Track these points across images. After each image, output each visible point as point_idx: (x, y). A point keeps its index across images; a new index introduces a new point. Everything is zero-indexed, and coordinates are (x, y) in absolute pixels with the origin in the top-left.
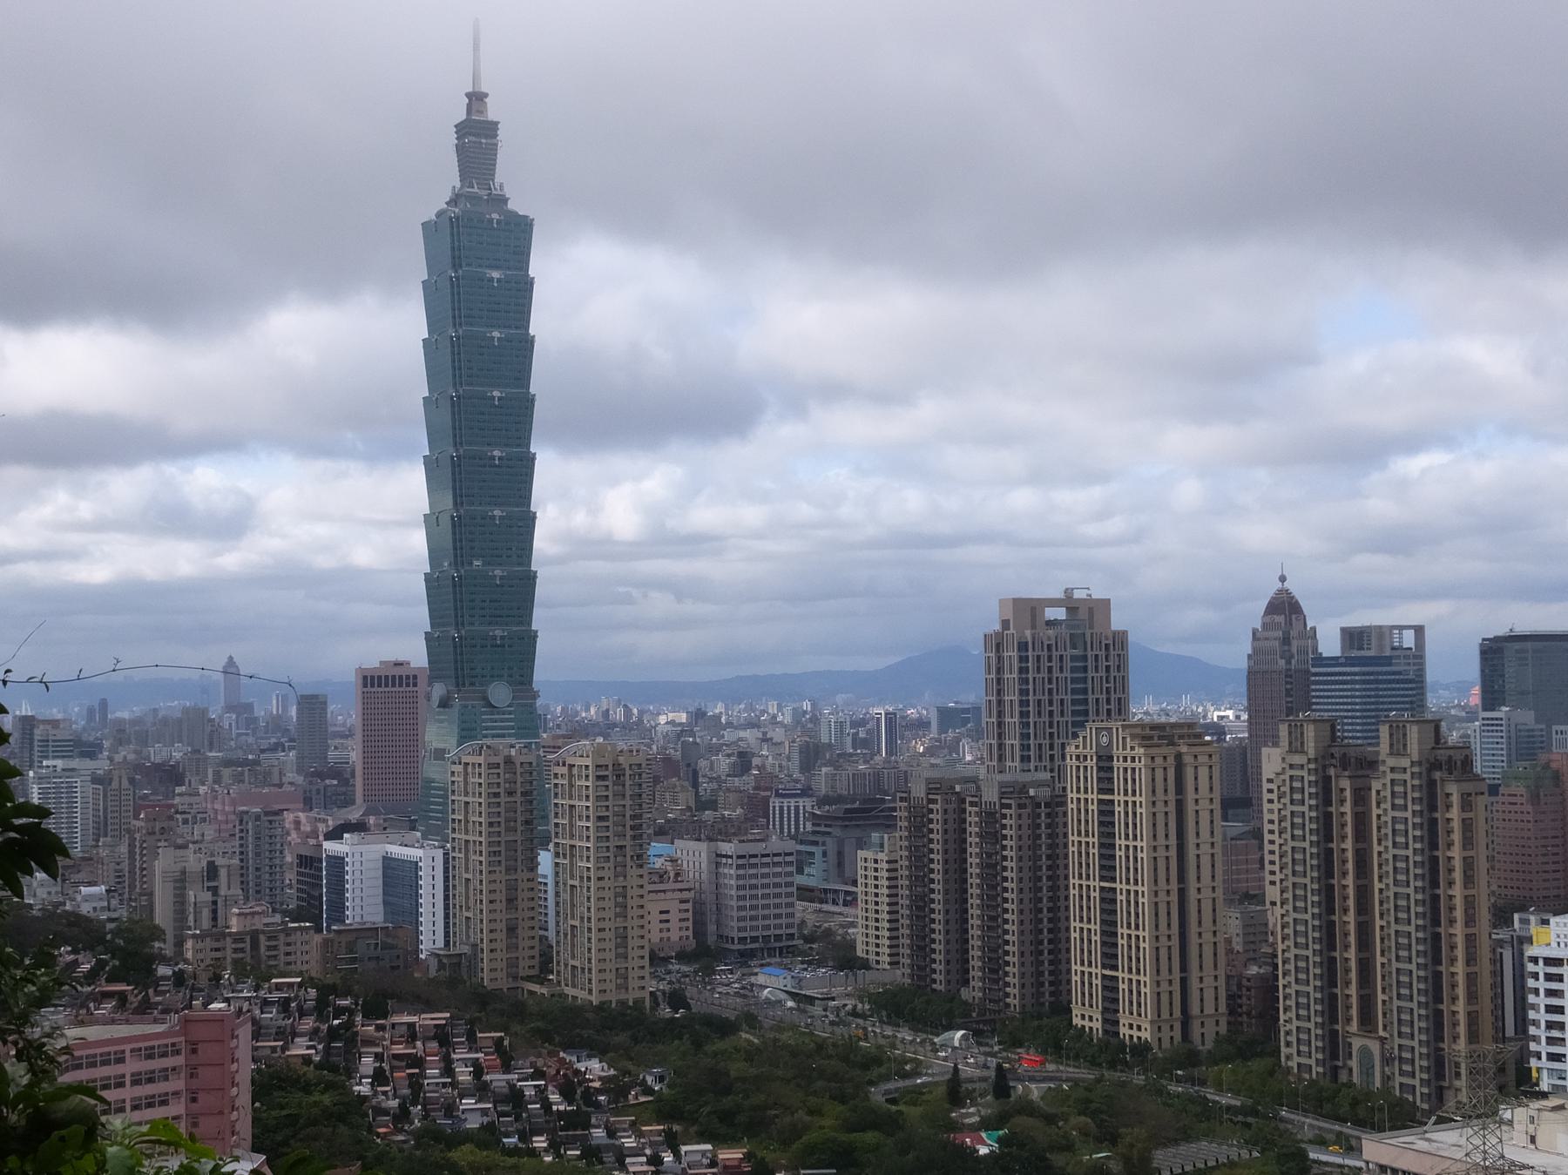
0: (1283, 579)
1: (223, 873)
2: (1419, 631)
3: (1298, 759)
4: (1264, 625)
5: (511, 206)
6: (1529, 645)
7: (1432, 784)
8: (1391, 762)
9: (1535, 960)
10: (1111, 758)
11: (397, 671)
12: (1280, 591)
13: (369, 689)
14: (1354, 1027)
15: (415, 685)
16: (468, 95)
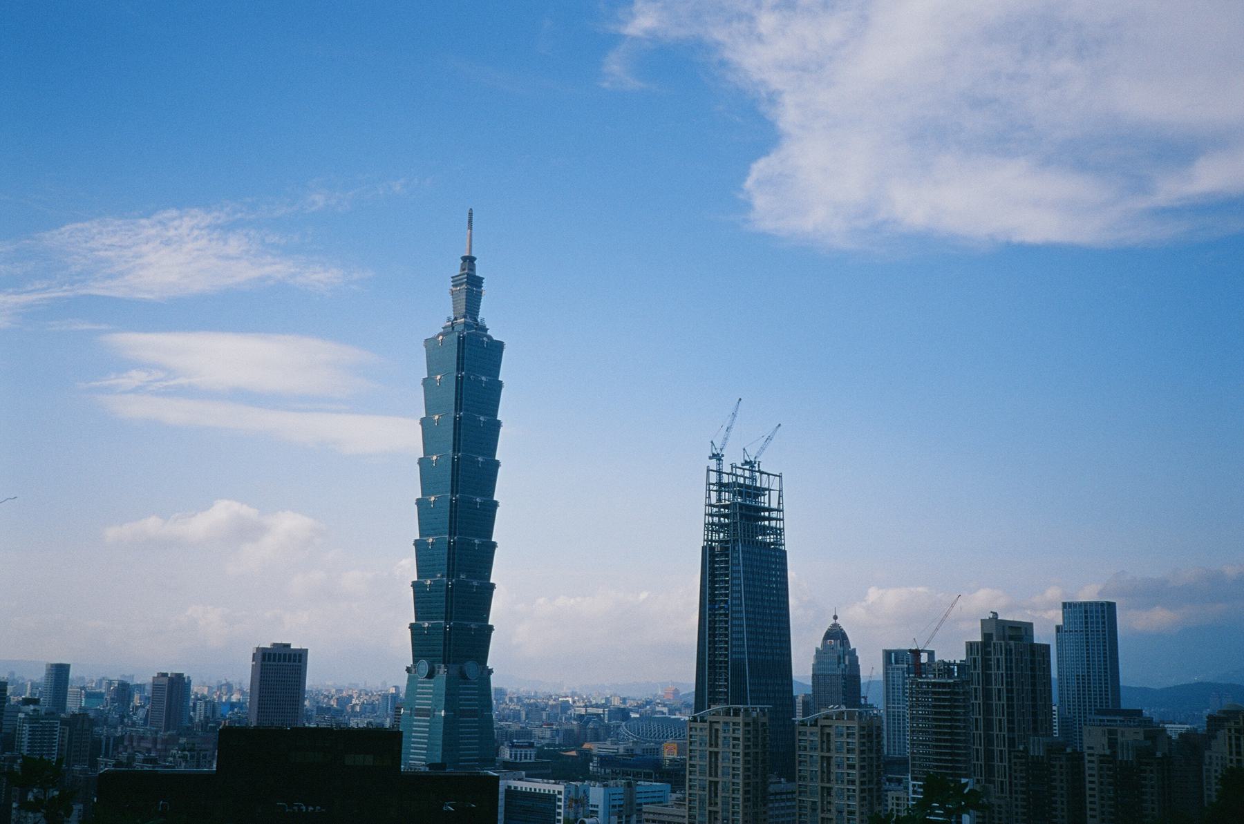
0: (835, 618)
2: (931, 654)
4: (824, 644)
5: (489, 333)
12: (835, 625)
16: (464, 259)
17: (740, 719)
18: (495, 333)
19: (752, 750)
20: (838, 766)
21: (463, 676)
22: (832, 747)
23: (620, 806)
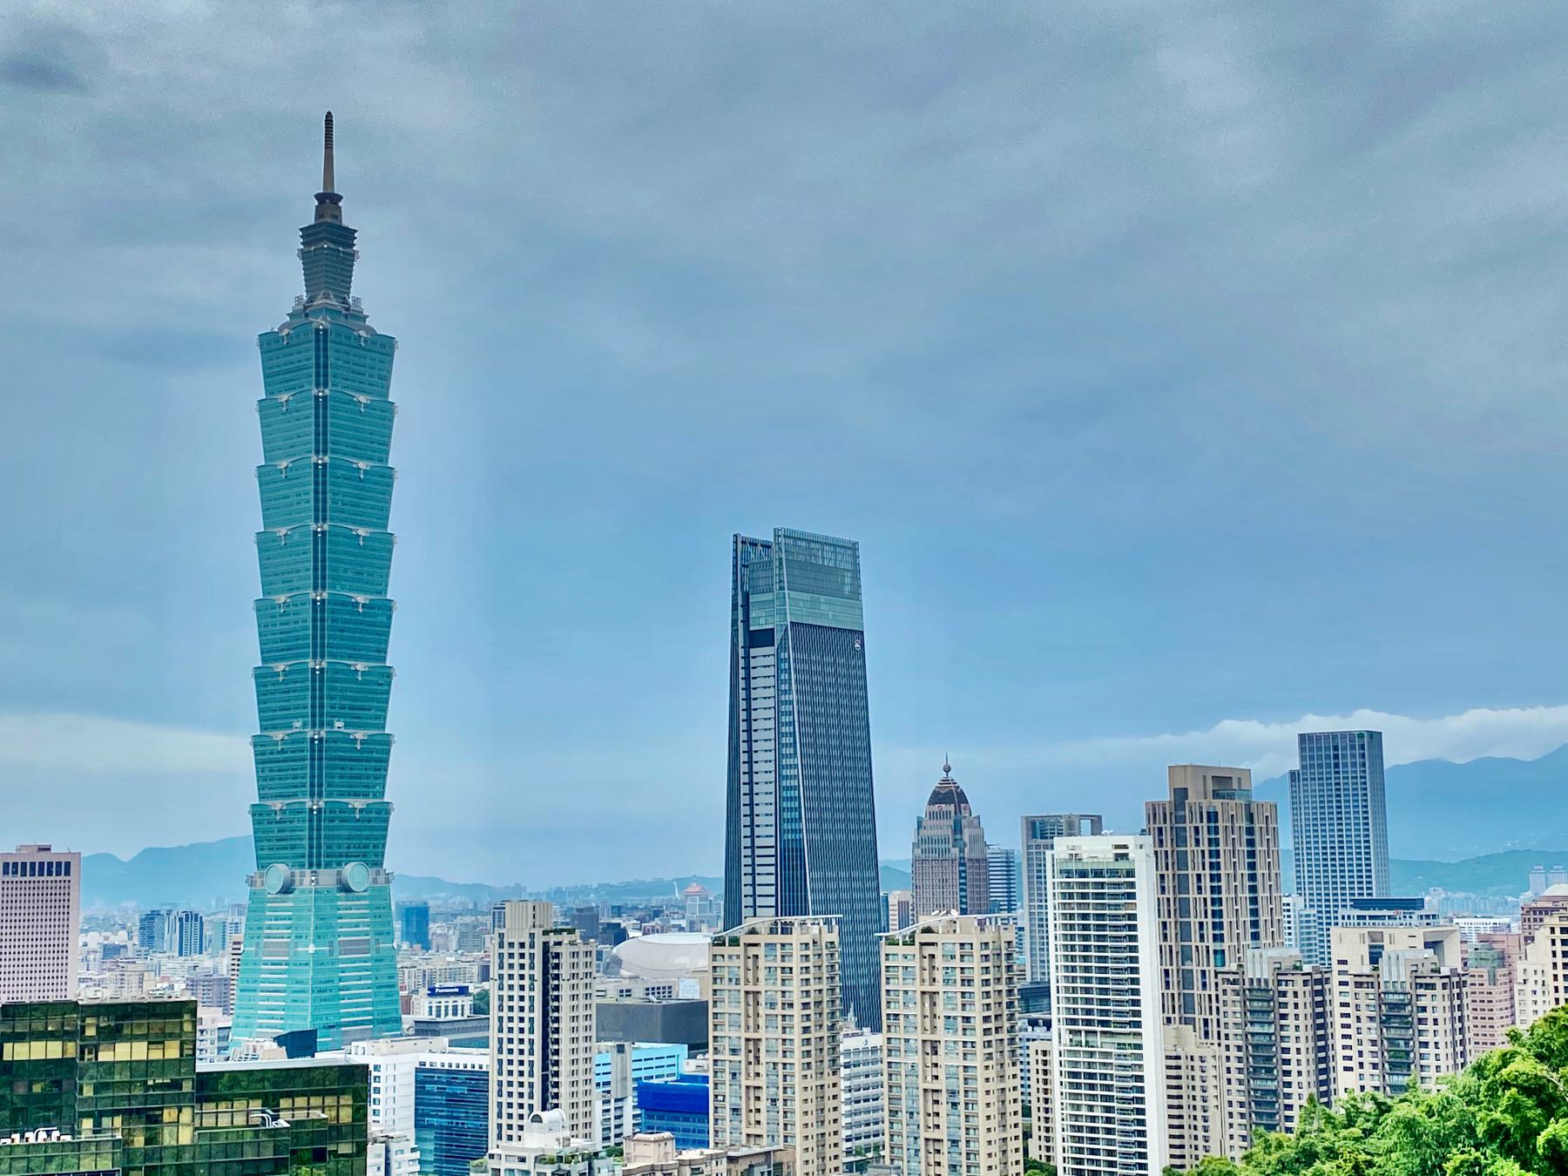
0: (947, 770)
4: (932, 815)
11: (45, 857)
12: (945, 781)
13: (10, 878)
15: (68, 873)
18: (379, 321)
19: (813, 987)
21: (346, 889)
22: (939, 975)
23: (608, 1083)
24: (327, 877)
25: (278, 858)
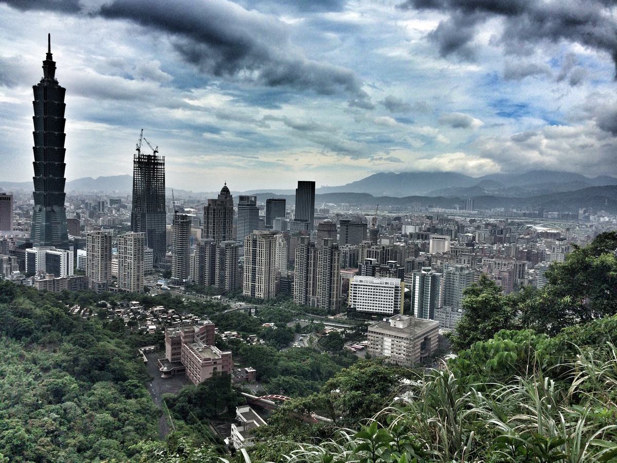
0: (225, 184)
1: (13, 260)
2: (255, 197)
3: (303, 245)
5: (59, 84)
6: (277, 202)
7: (332, 251)
8: (324, 247)
9: (352, 285)
10: (256, 241)
11: (4, 196)
14: (311, 295)
15: (9, 200)
17: (100, 236)
19: (105, 245)
20: (128, 250)
21: (53, 211)
24: (49, 209)
25: (39, 204)
